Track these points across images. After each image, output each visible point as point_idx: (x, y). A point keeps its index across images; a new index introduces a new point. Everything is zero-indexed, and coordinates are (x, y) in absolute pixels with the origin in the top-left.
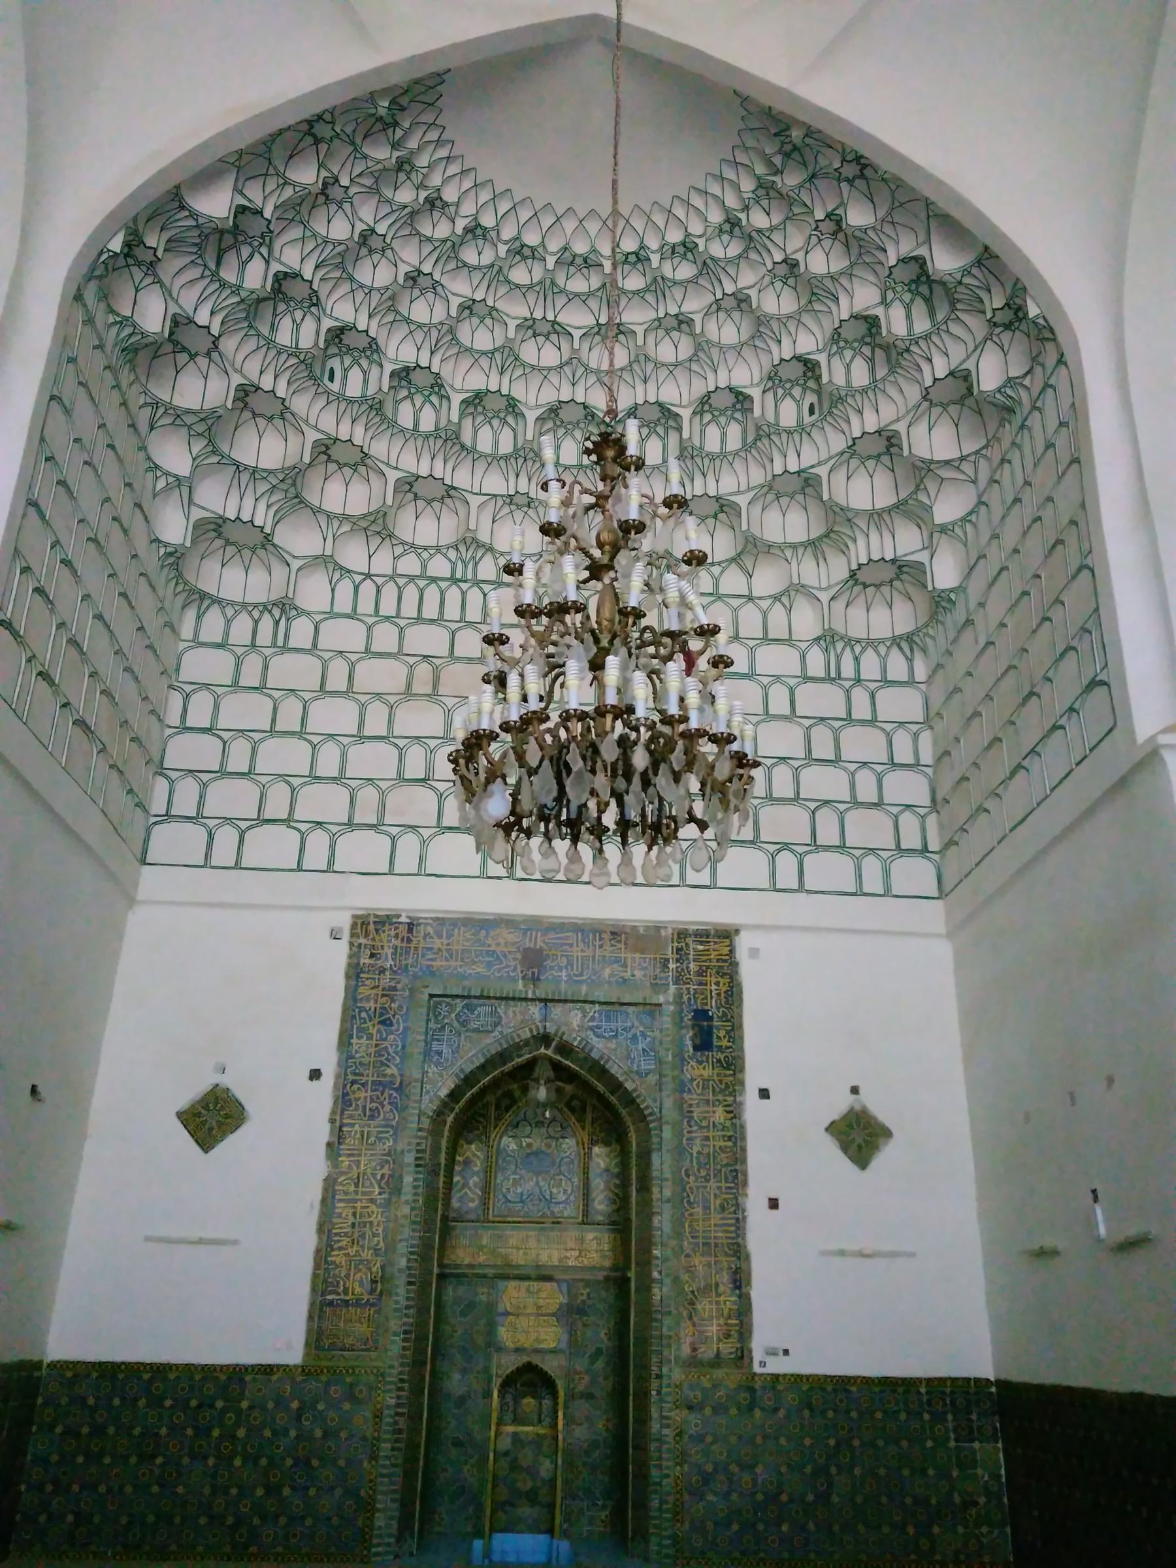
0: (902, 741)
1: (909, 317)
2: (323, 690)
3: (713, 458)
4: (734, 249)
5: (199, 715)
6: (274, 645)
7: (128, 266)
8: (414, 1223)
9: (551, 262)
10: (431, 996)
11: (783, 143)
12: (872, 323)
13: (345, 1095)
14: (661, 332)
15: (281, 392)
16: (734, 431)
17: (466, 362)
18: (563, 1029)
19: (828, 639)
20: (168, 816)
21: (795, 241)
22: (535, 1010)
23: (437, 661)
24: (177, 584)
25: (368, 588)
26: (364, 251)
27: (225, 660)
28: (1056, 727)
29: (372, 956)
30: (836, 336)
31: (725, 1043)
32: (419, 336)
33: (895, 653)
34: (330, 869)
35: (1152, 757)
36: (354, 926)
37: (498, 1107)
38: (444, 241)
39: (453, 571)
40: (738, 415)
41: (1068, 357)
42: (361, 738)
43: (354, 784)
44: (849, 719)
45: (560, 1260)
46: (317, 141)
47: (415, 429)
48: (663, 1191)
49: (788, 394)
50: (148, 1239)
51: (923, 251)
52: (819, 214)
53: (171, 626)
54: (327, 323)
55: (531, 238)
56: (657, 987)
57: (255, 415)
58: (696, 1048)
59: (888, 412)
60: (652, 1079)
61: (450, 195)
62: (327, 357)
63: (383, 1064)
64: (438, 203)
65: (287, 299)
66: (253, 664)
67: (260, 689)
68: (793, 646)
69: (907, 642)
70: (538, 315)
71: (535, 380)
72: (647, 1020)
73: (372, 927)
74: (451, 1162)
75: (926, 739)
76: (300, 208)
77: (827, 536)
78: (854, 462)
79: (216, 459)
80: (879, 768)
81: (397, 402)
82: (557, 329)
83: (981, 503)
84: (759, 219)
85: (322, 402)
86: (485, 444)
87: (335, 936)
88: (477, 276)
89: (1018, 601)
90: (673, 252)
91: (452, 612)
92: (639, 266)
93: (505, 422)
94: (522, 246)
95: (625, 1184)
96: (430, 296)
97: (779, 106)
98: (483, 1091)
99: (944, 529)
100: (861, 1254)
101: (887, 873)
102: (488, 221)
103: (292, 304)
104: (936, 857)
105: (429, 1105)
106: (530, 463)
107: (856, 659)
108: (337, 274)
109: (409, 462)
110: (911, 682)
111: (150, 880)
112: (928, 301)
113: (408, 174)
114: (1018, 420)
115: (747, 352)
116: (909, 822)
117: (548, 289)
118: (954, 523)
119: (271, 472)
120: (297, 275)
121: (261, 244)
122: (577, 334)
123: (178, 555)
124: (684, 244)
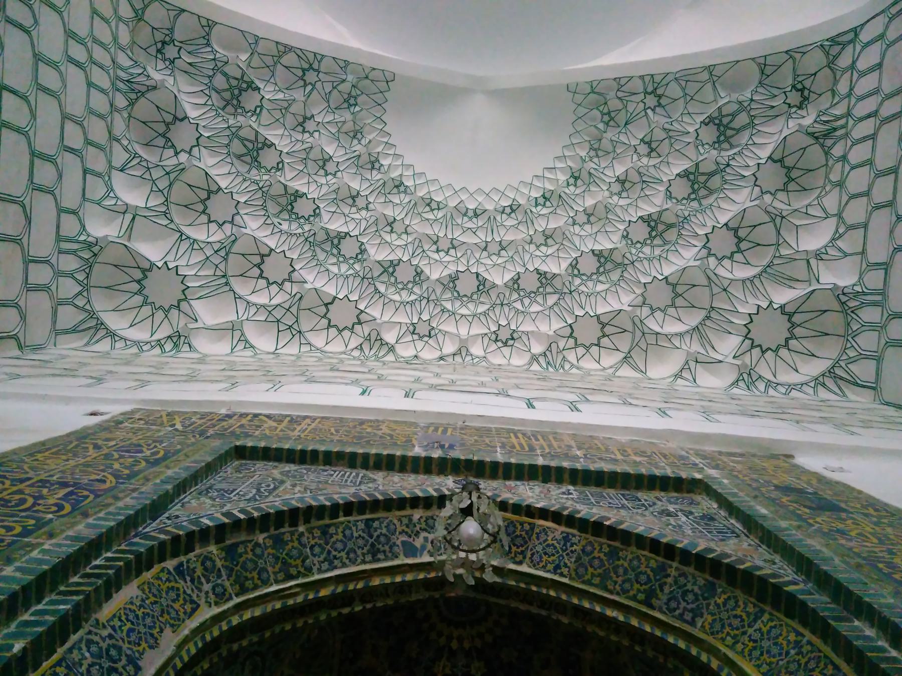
7: (156, 57)
11: (603, 114)
24: (80, 293)
40: (602, 278)
46: (305, 85)
57: (210, 221)
61: (385, 162)
64: (377, 165)
65: (259, 166)
70: (441, 235)
77: (708, 317)
79: (165, 222)
83: (839, 216)
88: (398, 210)
92: (513, 215)
94: (432, 200)
99: (818, 255)
102: (409, 183)
103: (263, 170)
106: (432, 305)
113: (359, 141)
121: (252, 115)
123: (96, 249)
124: (544, 196)
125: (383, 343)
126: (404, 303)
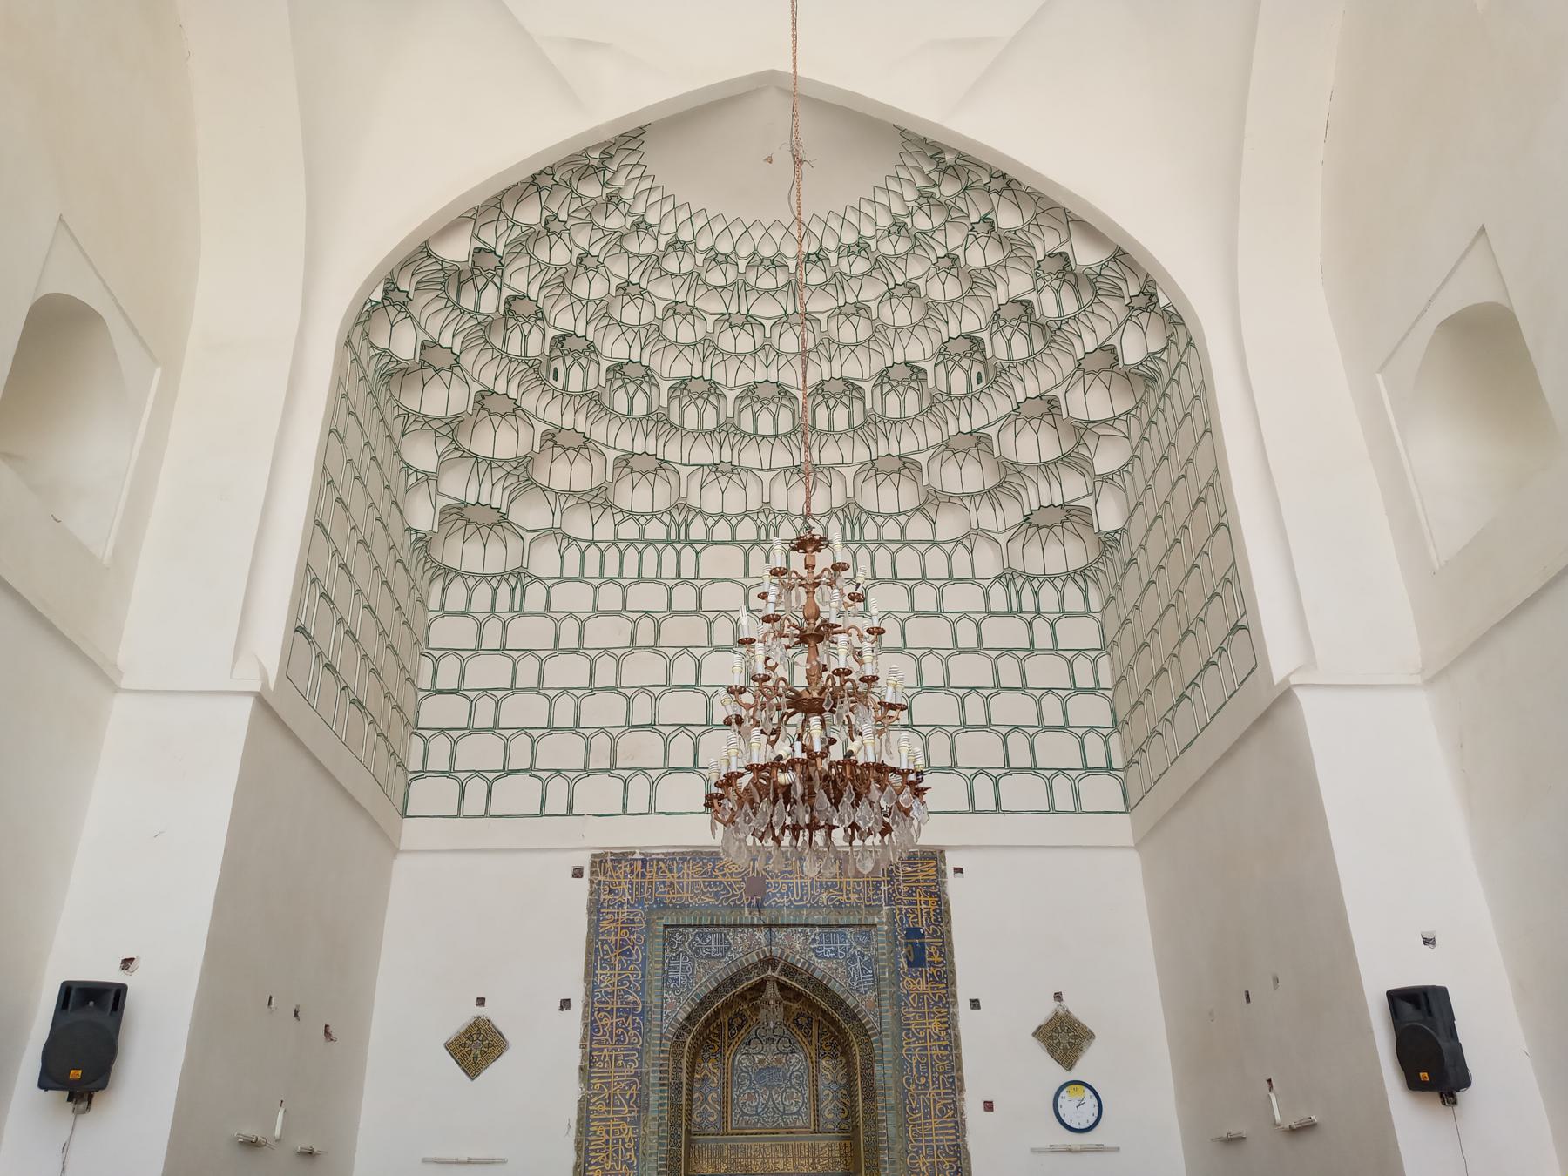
0: (1083, 668)
1: (1058, 300)
2: (558, 650)
3: (894, 422)
4: (903, 246)
5: (447, 679)
6: (512, 610)
8: (661, 1138)
9: (742, 265)
10: (666, 926)
12: (1027, 306)
13: (593, 1022)
14: (842, 318)
15: (513, 395)
16: (911, 397)
17: (672, 353)
18: (788, 951)
19: (1007, 577)
20: (424, 772)
21: (955, 238)
22: (761, 936)
23: (658, 616)
25: (593, 554)
26: (581, 269)
27: (469, 625)
28: (1210, 663)
29: (611, 891)
30: (996, 317)
31: (936, 959)
32: (630, 335)
33: (1070, 585)
34: (570, 812)
35: (1286, 696)
36: (593, 865)
37: (731, 1026)
38: (649, 256)
39: (668, 534)
41: (1195, 341)
42: (592, 690)
43: (587, 732)
44: (1032, 649)
45: (795, 1167)
46: (539, 190)
47: (630, 413)
48: (888, 1099)
49: (957, 364)
50: (425, 1161)
51: (1065, 248)
52: (974, 218)
53: (421, 601)
54: (551, 333)
55: (725, 247)
56: (873, 908)
58: (910, 964)
59: (1047, 380)
60: (871, 995)
61: (653, 218)
62: (550, 359)
63: (626, 992)
64: (643, 226)
65: (515, 316)
66: (493, 628)
67: (501, 650)
68: (977, 584)
69: (1080, 576)
70: (733, 310)
71: (734, 363)
72: (863, 939)
73: (609, 864)
74: (691, 1079)
75: (1104, 663)
76: (526, 242)
78: (1020, 422)
79: (458, 454)
80: (1063, 693)
81: (613, 392)
82: (750, 319)
84: (922, 222)
85: (548, 397)
86: (691, 422)
87: (578, 873)
88: (678, 282)
89: (1172, 546)
90: (848, 251)
91: (669, 570)
93: (708, 401)
95: (851, 1094)
96: (639, 302)
97: (932, 137)
98: (717, 1013)
99: (1105, 478)
100: (1070, 1151)
101: (1076, 792)
102: (686, 235)
104: (1121, 774)
105: (669, 1028)
107: (1035, 593)
108: (559, 291)
109: (625, 443)
110: (1087, 612)
111: (411, 832)
112: (1075, 287)
114: (1160, 386)
115: (917, 331)
116: (1093, 743)
117: (740, 287)
118: (1113, 473)
119: (506, 461)
120: (525, 296)
122: (768, 324)
125: (690, 509)
126: (701, 432)
